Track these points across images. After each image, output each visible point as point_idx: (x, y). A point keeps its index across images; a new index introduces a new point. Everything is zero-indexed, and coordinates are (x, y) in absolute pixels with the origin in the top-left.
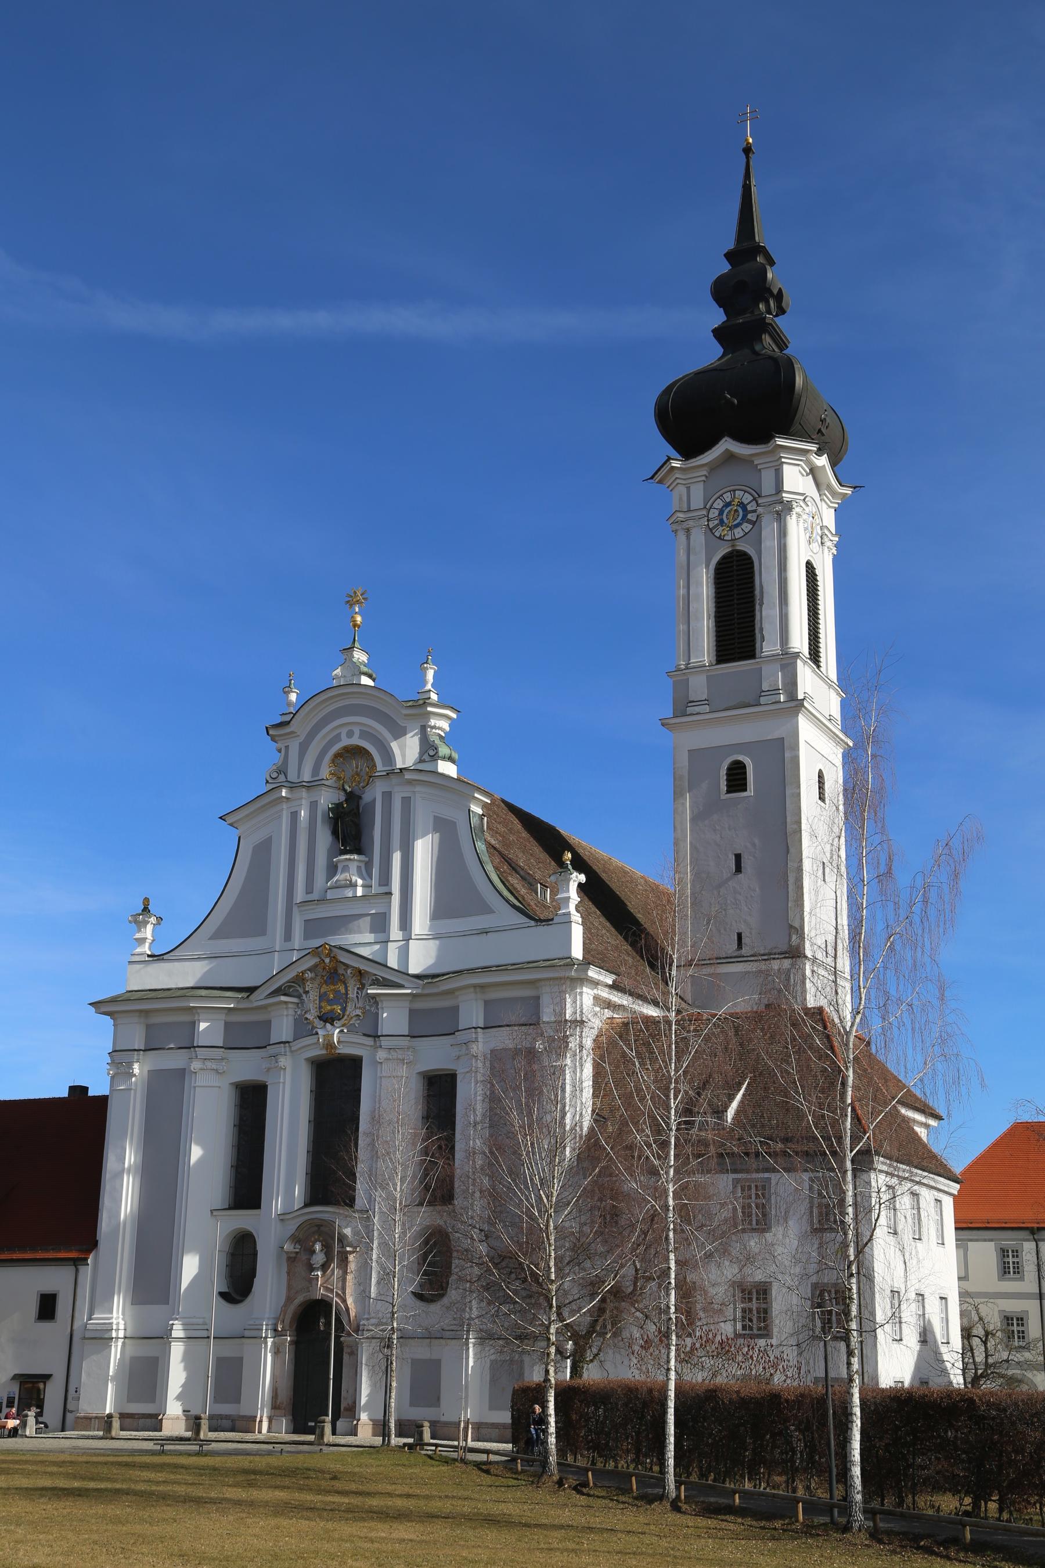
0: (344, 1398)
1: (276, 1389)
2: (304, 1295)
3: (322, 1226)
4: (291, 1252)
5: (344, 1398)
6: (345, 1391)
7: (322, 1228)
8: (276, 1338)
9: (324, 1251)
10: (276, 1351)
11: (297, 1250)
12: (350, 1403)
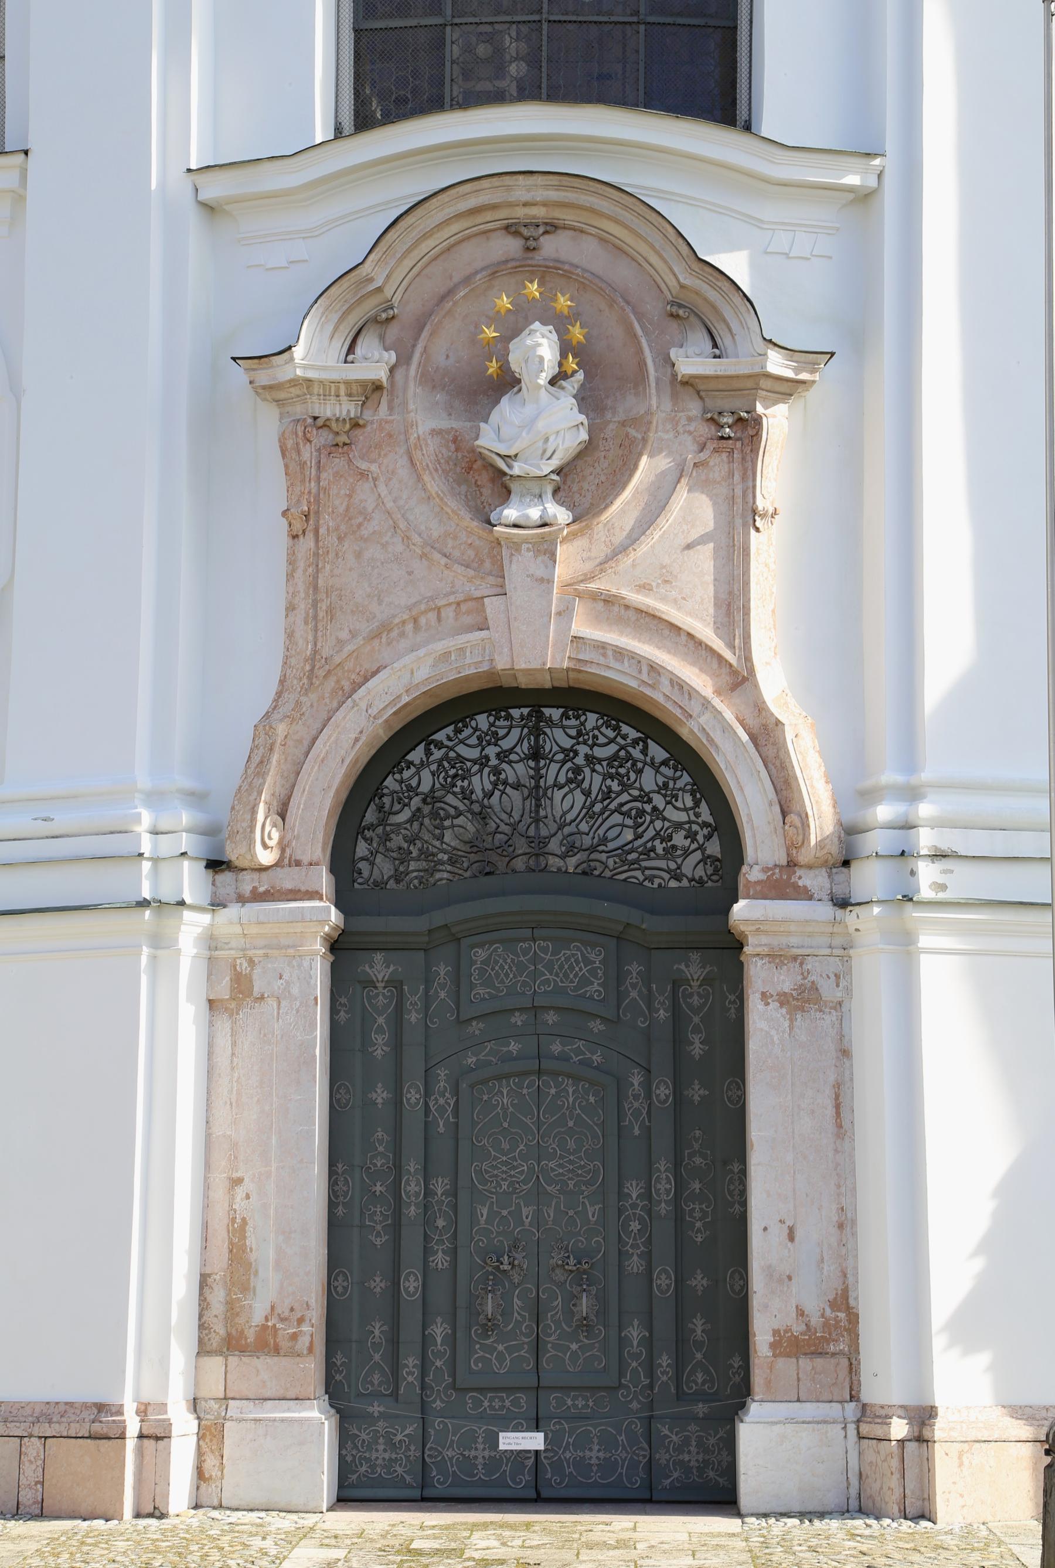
0: (769, 1271)
1: (238, 1230)
2: (440, 646)
3: (552, 227)
4: (329, 389)
5: (769, 1271)
6: (778, 1234)
7: (551, 246)
8: (233, 911)
9: (572, 385)
10: (223, 990)
11: (380, 373)
12: (815, 1305)
